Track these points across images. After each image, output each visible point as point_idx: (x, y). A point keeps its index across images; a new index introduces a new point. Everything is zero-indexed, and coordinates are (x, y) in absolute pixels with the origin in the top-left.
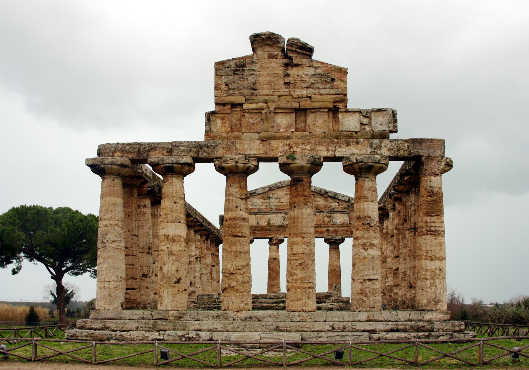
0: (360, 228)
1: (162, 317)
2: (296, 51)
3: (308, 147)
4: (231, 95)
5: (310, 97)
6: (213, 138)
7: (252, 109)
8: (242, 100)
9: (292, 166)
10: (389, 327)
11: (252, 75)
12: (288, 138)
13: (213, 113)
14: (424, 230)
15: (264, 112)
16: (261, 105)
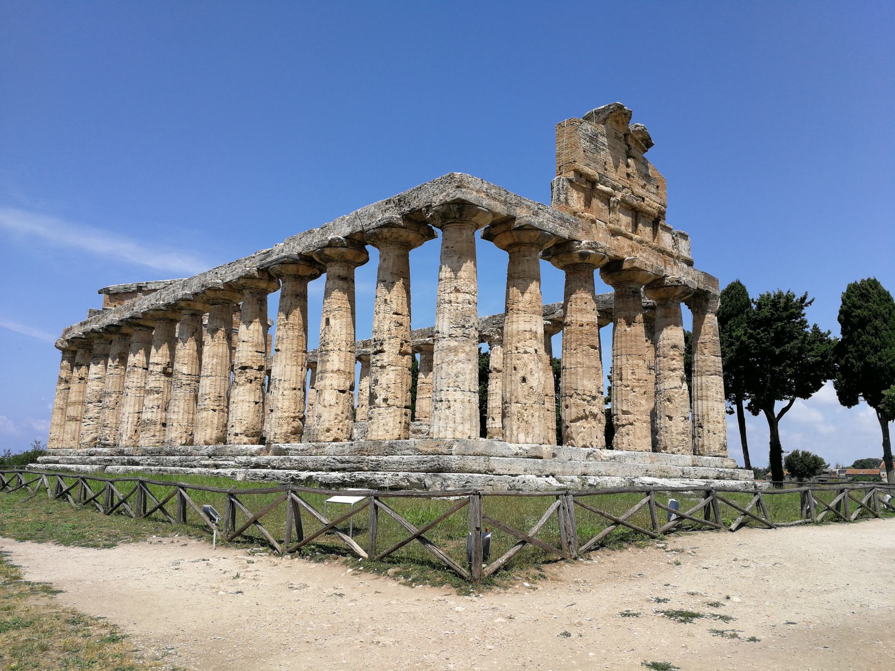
0: (678, 359)
1: (538, 454)
2: (636, 141)
3: (644, 255)
4: (588, 165)
5: (643, 199)
6: (575, 213)
7: (603, 192)
8: (597, 177)
9: (641, 273)
10: (715, 474)
11: (603, 150)
12: (631, 239)
13: (570, 181)
14: (712, 369)
15: (612, 199)
16: (609, 189)
